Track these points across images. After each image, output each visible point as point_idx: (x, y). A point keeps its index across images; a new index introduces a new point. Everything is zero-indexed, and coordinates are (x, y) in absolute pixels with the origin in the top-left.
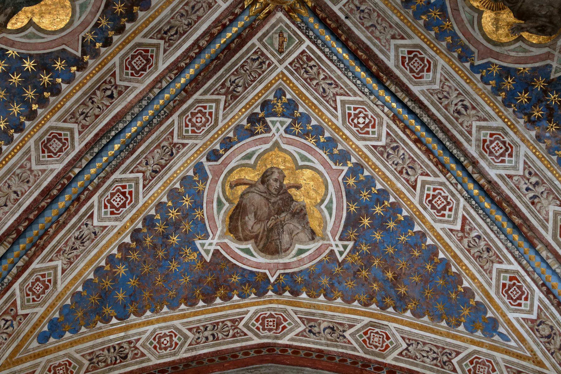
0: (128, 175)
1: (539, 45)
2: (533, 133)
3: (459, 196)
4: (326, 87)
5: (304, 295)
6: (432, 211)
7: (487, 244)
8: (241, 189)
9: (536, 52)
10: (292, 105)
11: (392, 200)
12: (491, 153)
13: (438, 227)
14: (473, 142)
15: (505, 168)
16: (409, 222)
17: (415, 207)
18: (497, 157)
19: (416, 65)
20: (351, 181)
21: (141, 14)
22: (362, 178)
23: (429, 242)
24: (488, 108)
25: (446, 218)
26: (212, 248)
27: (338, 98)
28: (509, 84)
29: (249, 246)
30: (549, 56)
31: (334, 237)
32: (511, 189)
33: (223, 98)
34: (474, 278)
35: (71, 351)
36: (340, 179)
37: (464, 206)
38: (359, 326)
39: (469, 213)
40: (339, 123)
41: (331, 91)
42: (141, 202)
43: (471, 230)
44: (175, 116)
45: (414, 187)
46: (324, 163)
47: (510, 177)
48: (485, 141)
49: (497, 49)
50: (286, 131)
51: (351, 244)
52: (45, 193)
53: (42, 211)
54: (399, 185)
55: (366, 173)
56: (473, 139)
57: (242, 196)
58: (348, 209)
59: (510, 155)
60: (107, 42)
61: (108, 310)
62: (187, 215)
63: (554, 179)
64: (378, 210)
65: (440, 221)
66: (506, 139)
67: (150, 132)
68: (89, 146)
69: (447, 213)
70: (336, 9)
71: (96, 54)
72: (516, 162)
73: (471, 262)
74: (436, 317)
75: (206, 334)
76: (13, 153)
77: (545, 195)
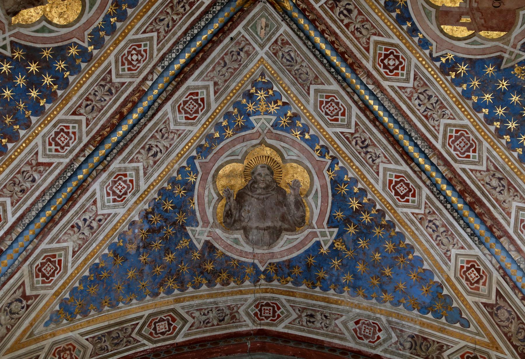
1: (215, 214)
2: (137, 218)
3: (71, 157)
4: (165, 22)
6: (53, 133)
7: (28, 190)
9: (209, 212)
11: (59, 93)
12: (115, 182)
13: (38, 140)
14: (123, 165)
15: (102, 197)
16: (39, 111)
17: (55, 116)
18: (111, 189)
19: (191, 107)
20: (73, 51)
22: (78, 62)
23: (22, 133)
24: (156, 175)
25: (48, 147)
27: (155, 34)
28: (180, 192)
30: (206, 223)
31: (14, 35)
32: (83, 205)
36: (75, 40)
37: (62, 163)
39: (56, 168)
40: (130, 36)
41: (162, 27)
43: (40, 172)
45: (74, 113)
46: (89, 23)
47: (95, 203)
48: (125, 175)
49: (210, 178)
54: (74, 99)
55: (83, 65)
56: (126, 165)
58: (44, 49)
59: (114, 201)
63: (97, 242)
64: (48, 80)
65: (44, 142)
66: (129, 195)
69: (53, 147)
70: (240, 28)
72: (109, 206)
73: (8, 175)
77: (82, 236)
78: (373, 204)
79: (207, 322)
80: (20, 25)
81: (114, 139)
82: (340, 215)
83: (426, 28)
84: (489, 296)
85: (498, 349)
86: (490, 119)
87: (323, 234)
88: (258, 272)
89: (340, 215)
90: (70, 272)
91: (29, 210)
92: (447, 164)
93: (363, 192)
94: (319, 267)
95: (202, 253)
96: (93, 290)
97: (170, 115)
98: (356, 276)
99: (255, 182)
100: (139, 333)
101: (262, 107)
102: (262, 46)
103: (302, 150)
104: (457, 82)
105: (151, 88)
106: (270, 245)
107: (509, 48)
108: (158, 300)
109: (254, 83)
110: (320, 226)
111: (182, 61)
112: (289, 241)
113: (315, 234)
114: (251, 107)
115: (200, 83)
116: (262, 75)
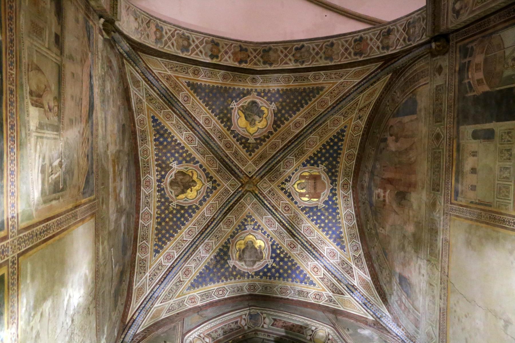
0: (197, 142)
1: (236, 256)
5: (158, 194)
8: (191, 174)
10: (215, 188)
13: (184, 233)
16: (184, 224)
19: (228, 223)
21: (241, 146)
23: (179, 231)
26: (173, 166)
28: (225, 249)
29: (173, 177)
33: (217, 169)
34: (170, 245)
35: (147, 125)
38: (150, 211)
40: (211, 202)
41: (219, 199)
42: (189, 146)
44: (213, 155)
46: (199, 198)
50: (208, 188)
51: (175, 207)
52: (194, 118)
53: (191, 118)
56: (209, 241)
57: (189, 175)
60: (234, 137)
61: (158, 136)
62: (184, 159)
64: (186, 215)
67: (209, 149)
68: (206, 131)
70: (242, 200)
71: (231, 134)
74: (157, 235)
75: (146, 165)
76: (206, 110)
78: (284, 251)
79: (234, 291)
80: (179, 199)
81: (206, 232)
82: (274, 255)
83: (296, 198)
84: (321, 275)
85: (325, 291)
86: (316, 224)
87: (269, 261)
88: (249, 275)
89: (274, 255)
90: (193, 274)
91: (181, 254)
92: (305, 237)
93: (281, 248)
94: (268, 272)
95: (232, 269)
96: (200, 280)
97: (222, 226)
98: (280, 273)
99: (247, 246)
100: (214, 294)
101: (249, 223)
102: (249, 205)
103: (262, 236)
104: (306, 213)
105: (217, 217)
106: (253, 266)
107: (320, 203)
108: (219, 284)
109: (247, 216)
110: (268, 258)
111: (226, 209)
112: (258, 264)
113: (266, 262)
114: (246, 223)
115: (230, 216)
116: (249, 213)
